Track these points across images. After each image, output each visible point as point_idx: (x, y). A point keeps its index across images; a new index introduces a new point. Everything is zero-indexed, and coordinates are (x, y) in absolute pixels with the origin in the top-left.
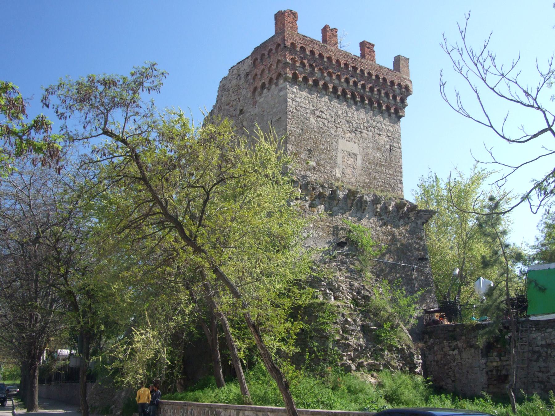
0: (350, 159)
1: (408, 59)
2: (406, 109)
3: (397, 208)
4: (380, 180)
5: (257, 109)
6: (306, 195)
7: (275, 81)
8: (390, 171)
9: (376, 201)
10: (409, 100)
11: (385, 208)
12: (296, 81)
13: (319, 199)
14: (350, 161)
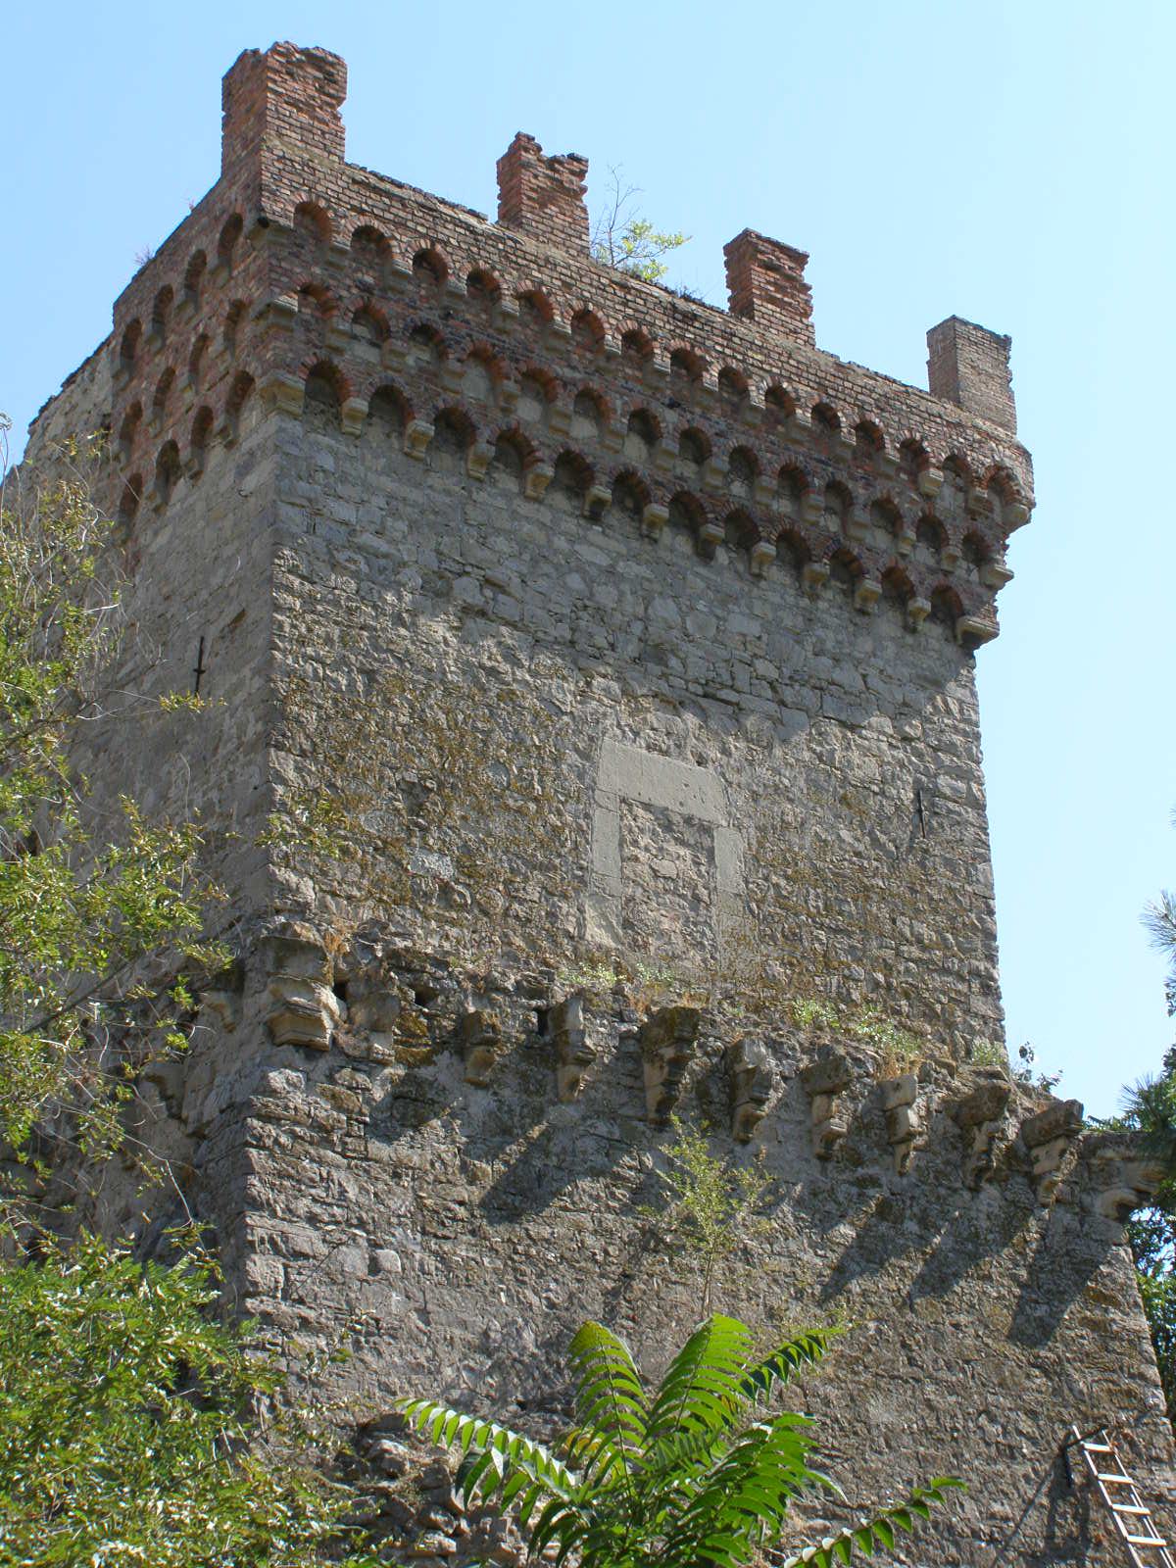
0: (672, 848)
1: (1003, 343)
2: (1003, 598)
3: (955, 1119)
4: (859, 971)
6: (376, 1028)
7: (218, 423)
8: (922, 929)
9: (825, 1076)
10: (1020, 549)
11: (882, 1123)
12: (338, 417)
13: (461, 1053)
14: (678, 861)
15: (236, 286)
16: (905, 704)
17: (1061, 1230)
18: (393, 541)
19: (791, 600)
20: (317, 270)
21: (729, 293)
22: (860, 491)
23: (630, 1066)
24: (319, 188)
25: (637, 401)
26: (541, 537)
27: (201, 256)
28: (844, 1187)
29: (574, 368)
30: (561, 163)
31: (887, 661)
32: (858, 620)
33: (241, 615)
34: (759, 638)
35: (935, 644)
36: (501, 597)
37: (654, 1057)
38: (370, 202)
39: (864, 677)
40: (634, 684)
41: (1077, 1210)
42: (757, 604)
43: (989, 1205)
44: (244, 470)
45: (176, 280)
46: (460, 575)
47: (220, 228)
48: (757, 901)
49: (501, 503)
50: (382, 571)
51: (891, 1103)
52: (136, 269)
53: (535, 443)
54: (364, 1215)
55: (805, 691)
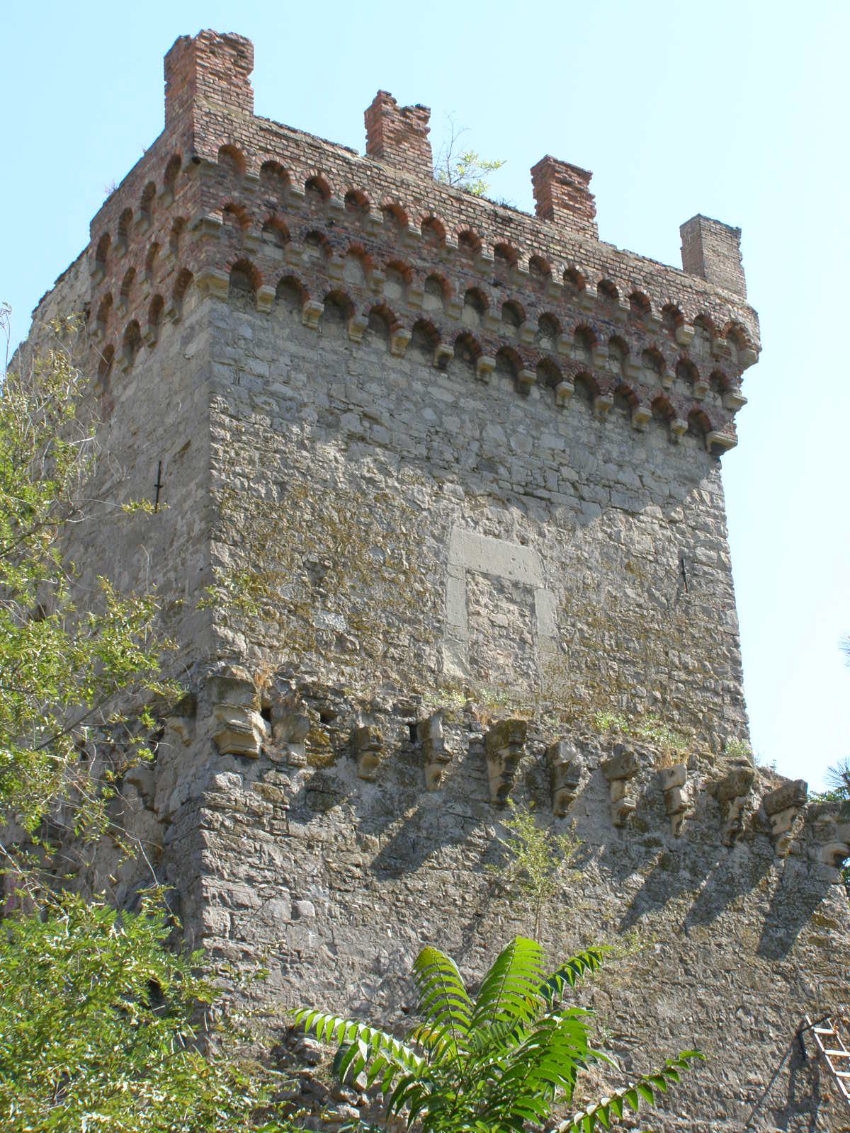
0: (504, 604)
1: (735, 233)
2: (740, 418)
3: (715, 796)
4: (642, 690)
5: (115, 432)
6: (293, 740)
7: (168, 306)
8: (688, 659)
9: (619, 767)
10: (751, 382)
11: (662, 800)
12: (253, 299)
13: (355, 757)
14: (509, 614)
15: (178, 207)
16: (671, 496)
17: (793, 874)
18: (296, 389)
19: (586, 423)
20: (236, 194)
21: (535, 202)
22: (634, 343)
23: (478, 763)
24: (235, 134)
25: (471, 283)
26: (403, 382)
27: (152, 186)
28: (635, 847)
29: (424, 259)
30: (411, 111)
31: (657, 466)
32: (635, 436)
33: (188, 445)
34: (564, 451)
35: (691, 452)
36: (376, 427)
37: (495, 757)
38: (273, 143)
39: (641, 477)
40: (474, 487)
41: (805, 859)
42: (562, 426)
43: (741, 857)
44: (187, 340)
45: (134, 204)
46: (345, 412)
47: (165, 166)
48: (567, 642)
49: (373, 358)
50: (289, 410)
51: (669, 784)
52: (105, 197)
53: (397, 315)
54: (287, 876)
55: (598, 488)
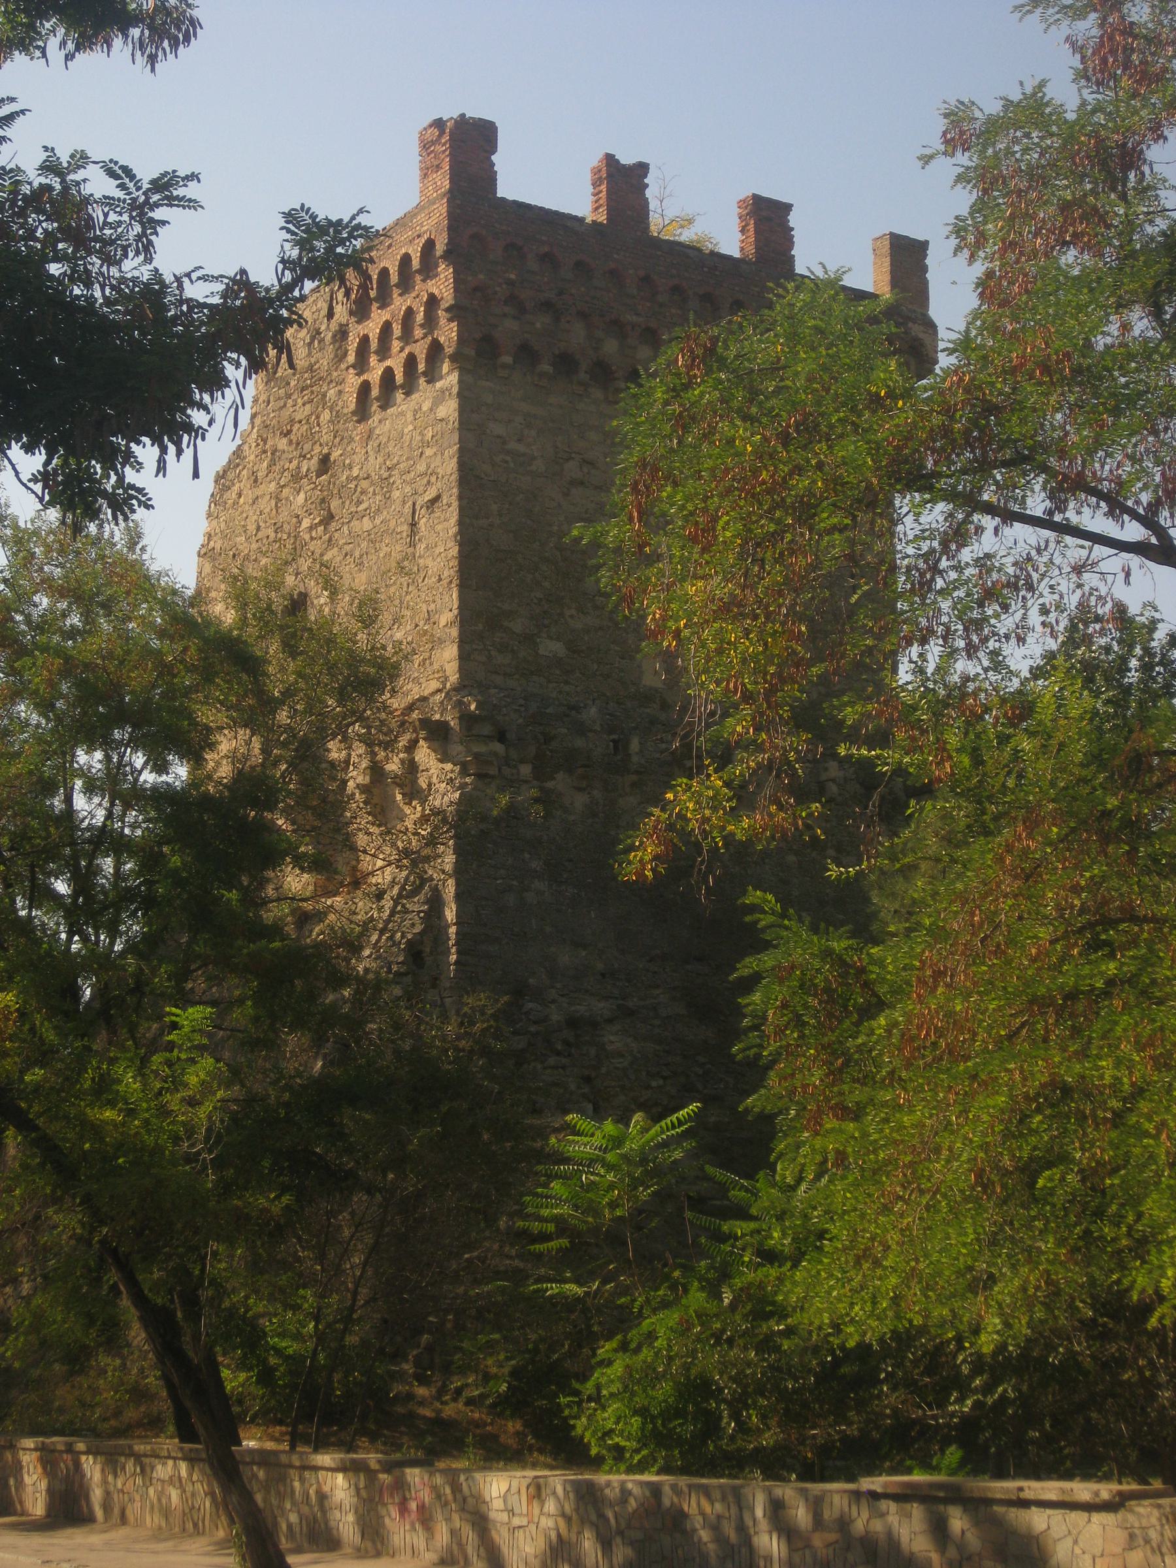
20: (481, 276)
46: (568, 460)
